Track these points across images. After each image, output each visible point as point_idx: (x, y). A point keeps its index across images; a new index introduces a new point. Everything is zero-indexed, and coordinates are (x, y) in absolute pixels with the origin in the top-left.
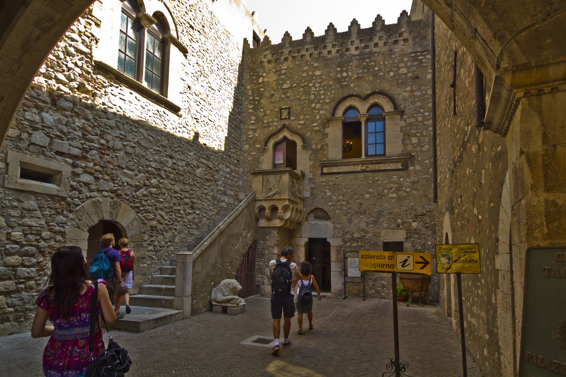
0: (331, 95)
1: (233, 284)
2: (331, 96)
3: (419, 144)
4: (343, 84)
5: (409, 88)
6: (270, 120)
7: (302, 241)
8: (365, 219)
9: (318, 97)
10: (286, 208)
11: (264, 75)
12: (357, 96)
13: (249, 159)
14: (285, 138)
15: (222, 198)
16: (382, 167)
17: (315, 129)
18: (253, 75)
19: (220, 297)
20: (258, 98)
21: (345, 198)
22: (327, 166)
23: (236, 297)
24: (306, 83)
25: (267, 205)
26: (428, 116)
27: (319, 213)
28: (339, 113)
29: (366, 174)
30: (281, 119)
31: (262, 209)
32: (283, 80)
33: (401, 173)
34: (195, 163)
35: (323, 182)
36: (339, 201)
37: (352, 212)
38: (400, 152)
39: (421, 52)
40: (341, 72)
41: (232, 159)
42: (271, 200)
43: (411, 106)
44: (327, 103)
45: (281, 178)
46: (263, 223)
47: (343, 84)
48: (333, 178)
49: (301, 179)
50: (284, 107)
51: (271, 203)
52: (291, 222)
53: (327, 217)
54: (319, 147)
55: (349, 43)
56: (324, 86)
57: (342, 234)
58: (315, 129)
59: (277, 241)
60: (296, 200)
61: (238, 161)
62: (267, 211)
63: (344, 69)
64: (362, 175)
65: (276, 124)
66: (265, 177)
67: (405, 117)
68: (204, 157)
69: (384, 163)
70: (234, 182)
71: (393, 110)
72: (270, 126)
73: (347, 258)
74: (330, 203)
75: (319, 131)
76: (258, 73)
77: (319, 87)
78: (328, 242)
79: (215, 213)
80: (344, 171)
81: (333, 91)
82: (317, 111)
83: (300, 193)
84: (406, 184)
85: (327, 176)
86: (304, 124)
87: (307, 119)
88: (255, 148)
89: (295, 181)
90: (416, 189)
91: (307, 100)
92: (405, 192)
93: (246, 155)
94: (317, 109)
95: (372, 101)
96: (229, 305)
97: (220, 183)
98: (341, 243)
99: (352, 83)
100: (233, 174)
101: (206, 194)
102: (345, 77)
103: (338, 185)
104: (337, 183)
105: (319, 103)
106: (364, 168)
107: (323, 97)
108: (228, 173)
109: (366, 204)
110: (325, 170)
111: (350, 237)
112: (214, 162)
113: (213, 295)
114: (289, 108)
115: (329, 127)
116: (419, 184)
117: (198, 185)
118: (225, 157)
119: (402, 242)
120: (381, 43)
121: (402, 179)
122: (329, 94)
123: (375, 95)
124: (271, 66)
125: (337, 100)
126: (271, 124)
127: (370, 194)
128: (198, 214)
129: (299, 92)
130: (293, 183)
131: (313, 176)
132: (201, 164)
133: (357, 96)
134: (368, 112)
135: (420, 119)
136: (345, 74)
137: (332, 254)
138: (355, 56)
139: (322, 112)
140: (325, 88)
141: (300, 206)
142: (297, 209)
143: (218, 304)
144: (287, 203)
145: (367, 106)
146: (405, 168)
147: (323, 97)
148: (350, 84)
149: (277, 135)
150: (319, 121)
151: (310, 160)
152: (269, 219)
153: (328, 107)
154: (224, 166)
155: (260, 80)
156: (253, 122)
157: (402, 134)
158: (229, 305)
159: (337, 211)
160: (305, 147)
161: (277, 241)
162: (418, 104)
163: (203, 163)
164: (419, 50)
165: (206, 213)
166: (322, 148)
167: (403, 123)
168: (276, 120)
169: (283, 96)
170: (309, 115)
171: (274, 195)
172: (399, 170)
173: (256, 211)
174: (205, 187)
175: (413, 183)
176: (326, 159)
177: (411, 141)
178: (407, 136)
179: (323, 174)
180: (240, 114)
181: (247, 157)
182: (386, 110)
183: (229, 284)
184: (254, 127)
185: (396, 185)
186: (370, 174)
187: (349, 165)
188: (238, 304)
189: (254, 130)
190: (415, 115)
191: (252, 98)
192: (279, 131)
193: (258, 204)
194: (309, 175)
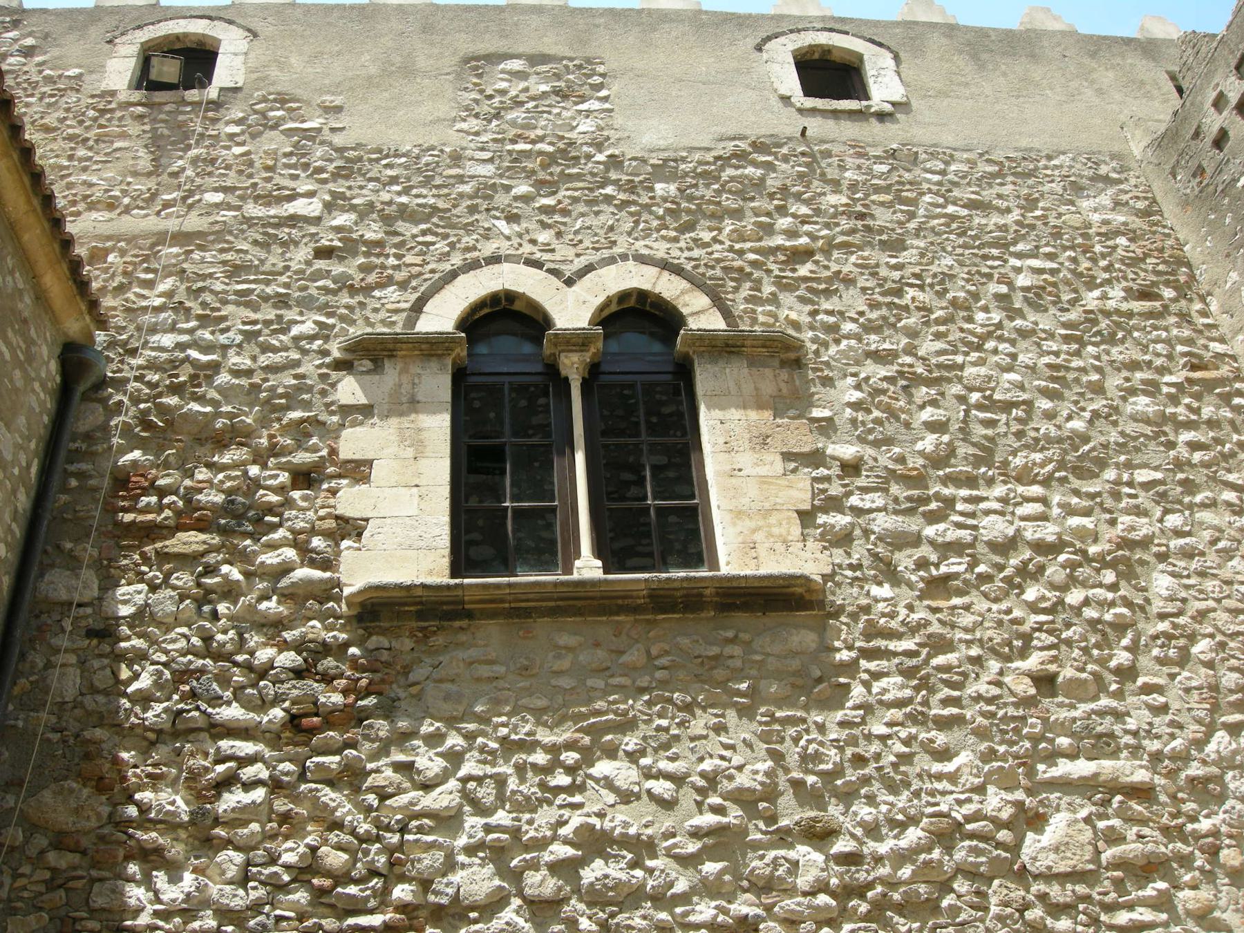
34: (996, 801)
112: (1153, 746)
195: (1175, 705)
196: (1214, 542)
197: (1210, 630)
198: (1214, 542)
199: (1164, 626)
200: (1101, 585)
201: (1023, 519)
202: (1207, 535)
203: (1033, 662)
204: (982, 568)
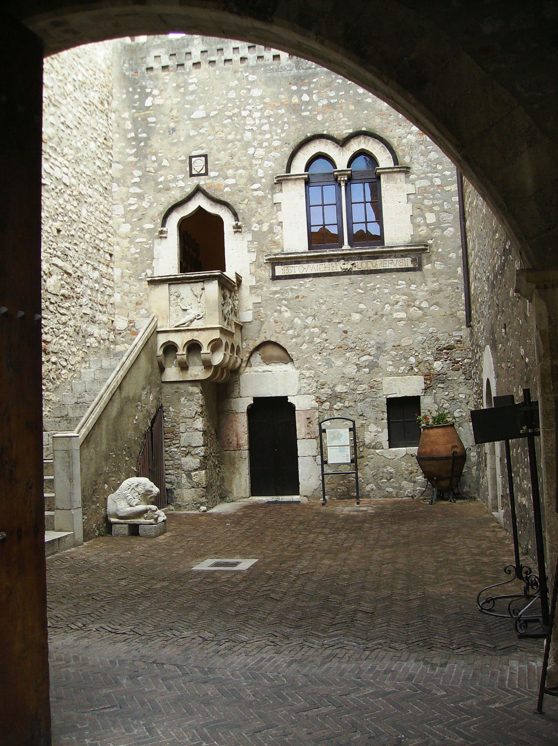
0: (282, 132)
1: (145, 485)
2: (282, 135)
3: (438, 225)
4: (304, 114)
6: (170, 177)
7: (243, 404)
8: (355, 359)
9: (259, 137)
10: (215, 345)
13: (133, 250)
14: (200, 210)
15: (89, 329)
17: (256, 193)
18: (134, 92)
19: (124, 508)
20: (144, 135)
21: (318, 323)
22: (281, 264)
23: (154, 507)
24: (236, 111)
25: (180, 340)
26: (451, 176)
27: (271, 351)
30: (192, 175)
31: (170, 348)
32: (192, 103)
33: (410, 274)
35: (275, 292)
37: (331, 347)
38: (408, 239)
40: (299, 93)
41: (102, 252)
42: (188, 330)
43: (421, 158)
45: (203, 289)
46: (172, 373)
47: (304, 114)
49: (236, 288)
50: (194, 153)
51: (188, 337)
52: (222, 370)
53: (287, 358)
54: (265, 227)
56: (269, 117)
57: (314, 388)
58: (256, 193)
59: (202, 406)
60: (229, 329)
61: (111, 255)
62: (182, 351)
63: (305, 88)
64: (345, 280)
66: (174, 288)
67: (412, 177)
68: (59, 254)
69: (382, 257)
70: (106, 298)
71: (392, 165)
72: (168, 189)
74: (291, 332)
75: (264, 197)
76: (143, 88)
77: (260, 118)
78: (291, 404)
79: (80, 358)
81: (286, 127)
83: (236, 315)
84: (420, 294)
86: (235, 185)
87: (241, 176)
88: (142, 230)
89: (228, 294)
90: (436, 304)
91: (239, 141)
92: (420, 308)
93: (125, 243)
95: (355, 146)
96: (142, 520)
97: (84, 300)
98: (315, 404)
99: (318, 113)
100: (105, 281)
101: (64, 324)
102: (308, 103)
103: (303, 297)
104: (301, 294)
105: (261, 147)
106: (348, 266)
107: (268, 136)
108: (96, 281)
109: (355, 332)
110: (280, 271)
111: (330, 392)
112: (74, 262)
113: (111, 508)
114: (206, 156)
116: (441, 294)
117: (51, 308)
118: (90, 250)
119: (419, 397)
121: (413, 287)
122: (279, 131)
123: (362, 138)
124: (166, 76)
125: (293, 144)
126: (172, 185)
127: (360, 313)
128: (54, 363)
129: (225, 126)
130: (224, 297)
131: (257, 282)
132: (55, 268)
134: (349, 166)
135: (438, 182)
136: (305, 98)
139: (267, 164)
140: (272, 120)
141: (237, 340)
142: (233, 345)
143: (122, 521)
144: (217, 335)
146: (418, 268)
147: (268, 136)
148: (316, 115)
149: (185, 206)
150: (263, 180)
151: (249, 251)
152: (184, 367)
153: (278, 155)
154: (90, 266)
155: (148, 102)
156: (138, 180)
157: (410, 206)
158: (142, 520)
159: (304, 347)
160: (238, 229)
161: (202, 406)
163: (57, 266)
165: (66, 360)
166: (271, 230)
168: (181, 176)
169: (193, 133)
170: (244, 168)
171: (191, 321)
172: (408, 270)
173: (160, 352)
174: (62, 311)
175: (433, 292)
176: (279, 251)
177: (425, 219)
178: (419, 210)
179: (275, 278)
180: (111, 166)
181: (129, 248)
182: (382, 165)
183: (137, 486)
184: (138, 190)
185: (404, 297)
186: (359, 278)
187: (322, 261)
188: (156, 519)
189: (140, 197)
190: (430, 175)
191: (133, 135)
193: (162, 339)
194: (248, 281)
195: (79, 252)
196: (95, 203)
197: (89, 232)
198: (95, 203)
199: (82, 226)
200: (72, 205)
201: (64, 173)
202: (95, 200)
203: (58, 225)
204: (53, 186)
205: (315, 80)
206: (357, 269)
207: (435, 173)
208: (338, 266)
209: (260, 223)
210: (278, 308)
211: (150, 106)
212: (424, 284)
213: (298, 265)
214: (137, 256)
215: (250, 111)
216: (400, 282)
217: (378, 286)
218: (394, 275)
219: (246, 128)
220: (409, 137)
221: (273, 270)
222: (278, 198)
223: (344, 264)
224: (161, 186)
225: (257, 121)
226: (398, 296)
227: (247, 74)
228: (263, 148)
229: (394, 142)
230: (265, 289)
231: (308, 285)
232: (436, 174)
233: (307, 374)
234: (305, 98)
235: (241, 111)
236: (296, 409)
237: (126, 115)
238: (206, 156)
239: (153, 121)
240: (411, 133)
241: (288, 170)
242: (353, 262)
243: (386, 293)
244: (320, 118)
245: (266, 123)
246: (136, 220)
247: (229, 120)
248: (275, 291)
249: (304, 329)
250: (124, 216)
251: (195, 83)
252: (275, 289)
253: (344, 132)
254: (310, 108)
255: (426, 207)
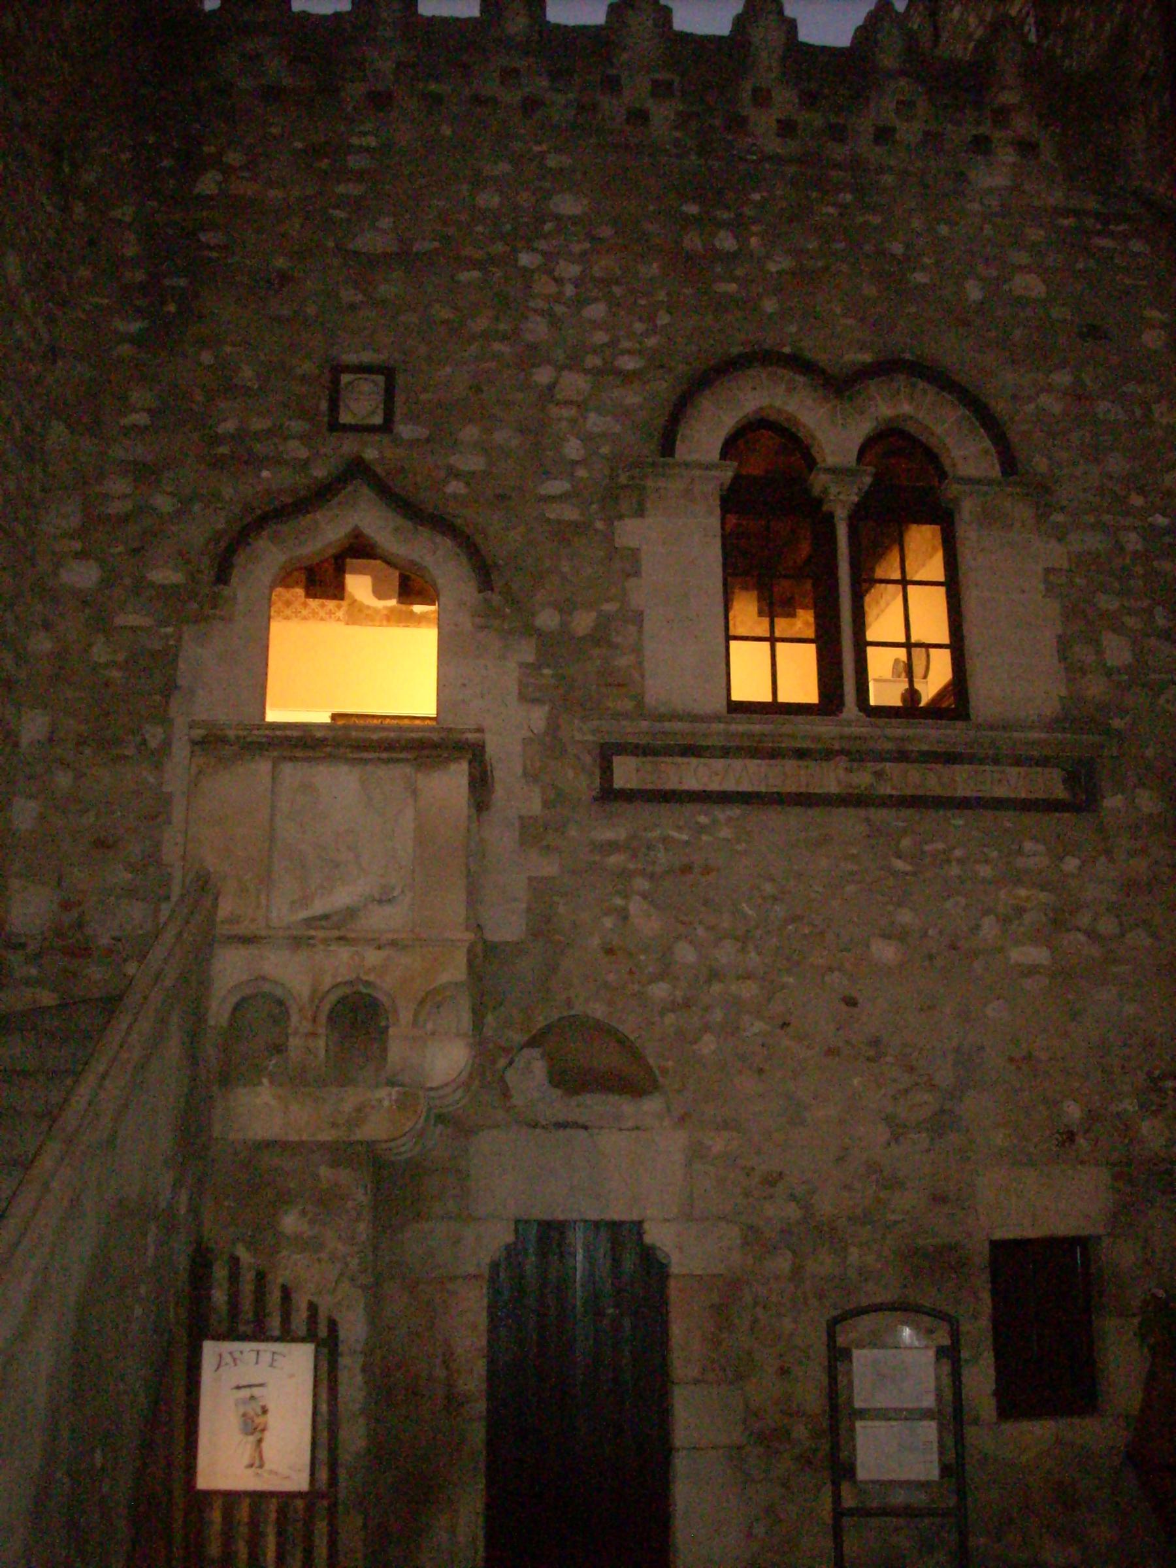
0: (646, 334)
2: (651, 342)
5: (1063, 378)
6: (258, 424)
11: (234, 158)
12: (799, 364)
16: (962, 781)
24: (499, 248)
28: (706, 434)
29: (879, 815)
30: (334, 426)
35: (612, 847)
36: (715, 975)
38: (1051, 708)
39: (1106, 220)
44: (627, 378)
48: (668, 824)
50: (350, 358)
51: (339, 964)
54: (583, 622)
55: (746, 96)
58: (553, 512)
64: (849, 822)
65: (297, 450)
69: (971, 759)
71: (996, 472)
72: (254, 462)
73: (846, 1354)
75: (581, 528)
80: (746, 787)
81: (663, 319)
82: (566, 413)
85: (646, 813)
88: (139, 586)
91: (504, 338)
92: (1092, 935)
94: (568, 403)
102: (733, 257)
106: (862, 779)
107: (600, 337)
110: (626, 772)
114: (389, 372)
115: (640, 513)
120: (909, 132)
121: (1071, 864)
131: (546, 804)
133: (799, 364)
136: (726, 242)
137: (676, 1331)
138: (779, 160)
139: (595, 422)
145: (860, 430)
150: (582, 473)
155: (208, 184)
156: (142, 419)
157: (1053, 608)
162: (1116, 464)
164: (1092, 204)
166: (600, 637)
167: (1055, 554)
172: (1051, 806)
179: (608, 795)
185: (1043, 896)
187: (774, 754)
192: (321, 495)
205: (757, 197)
206: (889, 791)
207: (1128, 514)
208: (830, 778)
209: (566, 608)
210: (619, 902)
211: (211, 198)
212: (1102, 859)
213: (694, 761)
214: (116, 674)
215: (544, 254)
216: (1028, 846)
217: (958, 853)
218: (1008, 820)
219: (531, 304)
220: (1044, 399)
221: (607, 770)
222: (630, 533)
223: (849, 770)
224: (224, 450)
225: (569, 290)
226: (1023, 892)
227: (544, 147)
228: (586, 372)
229: (1000, 407)
230: (573, 833)
231: (725, 833)
232: (1128, 522)
233: (718, 1143)
234: (726, 242)
235: (515, 251)
236: (675, 1270)
237: (125, 212)
238: (389, 372)
239: (213, 242)
240: (1049, 389)
241: (667, 446)
242: (879, 766)
243: (983, 881)
244: (770, 305)
245: (596, 300)
246: (121, 549)
247: (476, 274)
248: (610, 843)
249: (708, 981)
250: (81, 533)
251: (368, 150)
252: (609, 835)
253: (848, 357)
254: (739, 272)
255: (1102, 615)
